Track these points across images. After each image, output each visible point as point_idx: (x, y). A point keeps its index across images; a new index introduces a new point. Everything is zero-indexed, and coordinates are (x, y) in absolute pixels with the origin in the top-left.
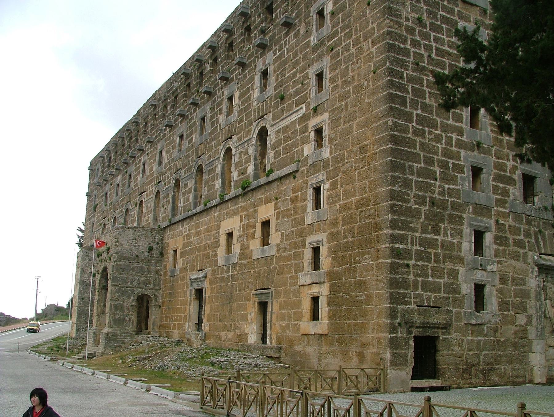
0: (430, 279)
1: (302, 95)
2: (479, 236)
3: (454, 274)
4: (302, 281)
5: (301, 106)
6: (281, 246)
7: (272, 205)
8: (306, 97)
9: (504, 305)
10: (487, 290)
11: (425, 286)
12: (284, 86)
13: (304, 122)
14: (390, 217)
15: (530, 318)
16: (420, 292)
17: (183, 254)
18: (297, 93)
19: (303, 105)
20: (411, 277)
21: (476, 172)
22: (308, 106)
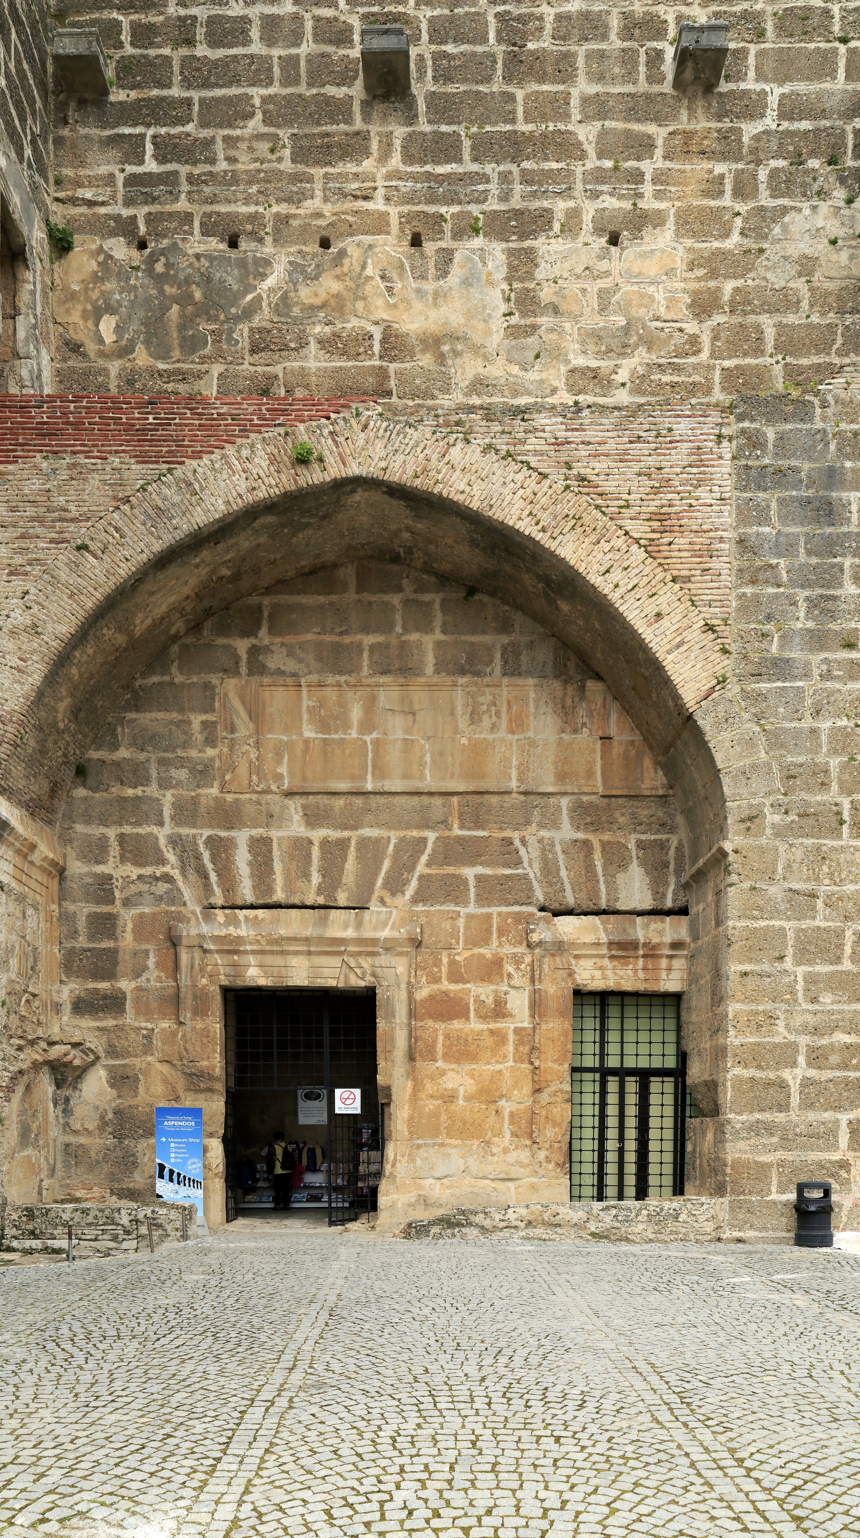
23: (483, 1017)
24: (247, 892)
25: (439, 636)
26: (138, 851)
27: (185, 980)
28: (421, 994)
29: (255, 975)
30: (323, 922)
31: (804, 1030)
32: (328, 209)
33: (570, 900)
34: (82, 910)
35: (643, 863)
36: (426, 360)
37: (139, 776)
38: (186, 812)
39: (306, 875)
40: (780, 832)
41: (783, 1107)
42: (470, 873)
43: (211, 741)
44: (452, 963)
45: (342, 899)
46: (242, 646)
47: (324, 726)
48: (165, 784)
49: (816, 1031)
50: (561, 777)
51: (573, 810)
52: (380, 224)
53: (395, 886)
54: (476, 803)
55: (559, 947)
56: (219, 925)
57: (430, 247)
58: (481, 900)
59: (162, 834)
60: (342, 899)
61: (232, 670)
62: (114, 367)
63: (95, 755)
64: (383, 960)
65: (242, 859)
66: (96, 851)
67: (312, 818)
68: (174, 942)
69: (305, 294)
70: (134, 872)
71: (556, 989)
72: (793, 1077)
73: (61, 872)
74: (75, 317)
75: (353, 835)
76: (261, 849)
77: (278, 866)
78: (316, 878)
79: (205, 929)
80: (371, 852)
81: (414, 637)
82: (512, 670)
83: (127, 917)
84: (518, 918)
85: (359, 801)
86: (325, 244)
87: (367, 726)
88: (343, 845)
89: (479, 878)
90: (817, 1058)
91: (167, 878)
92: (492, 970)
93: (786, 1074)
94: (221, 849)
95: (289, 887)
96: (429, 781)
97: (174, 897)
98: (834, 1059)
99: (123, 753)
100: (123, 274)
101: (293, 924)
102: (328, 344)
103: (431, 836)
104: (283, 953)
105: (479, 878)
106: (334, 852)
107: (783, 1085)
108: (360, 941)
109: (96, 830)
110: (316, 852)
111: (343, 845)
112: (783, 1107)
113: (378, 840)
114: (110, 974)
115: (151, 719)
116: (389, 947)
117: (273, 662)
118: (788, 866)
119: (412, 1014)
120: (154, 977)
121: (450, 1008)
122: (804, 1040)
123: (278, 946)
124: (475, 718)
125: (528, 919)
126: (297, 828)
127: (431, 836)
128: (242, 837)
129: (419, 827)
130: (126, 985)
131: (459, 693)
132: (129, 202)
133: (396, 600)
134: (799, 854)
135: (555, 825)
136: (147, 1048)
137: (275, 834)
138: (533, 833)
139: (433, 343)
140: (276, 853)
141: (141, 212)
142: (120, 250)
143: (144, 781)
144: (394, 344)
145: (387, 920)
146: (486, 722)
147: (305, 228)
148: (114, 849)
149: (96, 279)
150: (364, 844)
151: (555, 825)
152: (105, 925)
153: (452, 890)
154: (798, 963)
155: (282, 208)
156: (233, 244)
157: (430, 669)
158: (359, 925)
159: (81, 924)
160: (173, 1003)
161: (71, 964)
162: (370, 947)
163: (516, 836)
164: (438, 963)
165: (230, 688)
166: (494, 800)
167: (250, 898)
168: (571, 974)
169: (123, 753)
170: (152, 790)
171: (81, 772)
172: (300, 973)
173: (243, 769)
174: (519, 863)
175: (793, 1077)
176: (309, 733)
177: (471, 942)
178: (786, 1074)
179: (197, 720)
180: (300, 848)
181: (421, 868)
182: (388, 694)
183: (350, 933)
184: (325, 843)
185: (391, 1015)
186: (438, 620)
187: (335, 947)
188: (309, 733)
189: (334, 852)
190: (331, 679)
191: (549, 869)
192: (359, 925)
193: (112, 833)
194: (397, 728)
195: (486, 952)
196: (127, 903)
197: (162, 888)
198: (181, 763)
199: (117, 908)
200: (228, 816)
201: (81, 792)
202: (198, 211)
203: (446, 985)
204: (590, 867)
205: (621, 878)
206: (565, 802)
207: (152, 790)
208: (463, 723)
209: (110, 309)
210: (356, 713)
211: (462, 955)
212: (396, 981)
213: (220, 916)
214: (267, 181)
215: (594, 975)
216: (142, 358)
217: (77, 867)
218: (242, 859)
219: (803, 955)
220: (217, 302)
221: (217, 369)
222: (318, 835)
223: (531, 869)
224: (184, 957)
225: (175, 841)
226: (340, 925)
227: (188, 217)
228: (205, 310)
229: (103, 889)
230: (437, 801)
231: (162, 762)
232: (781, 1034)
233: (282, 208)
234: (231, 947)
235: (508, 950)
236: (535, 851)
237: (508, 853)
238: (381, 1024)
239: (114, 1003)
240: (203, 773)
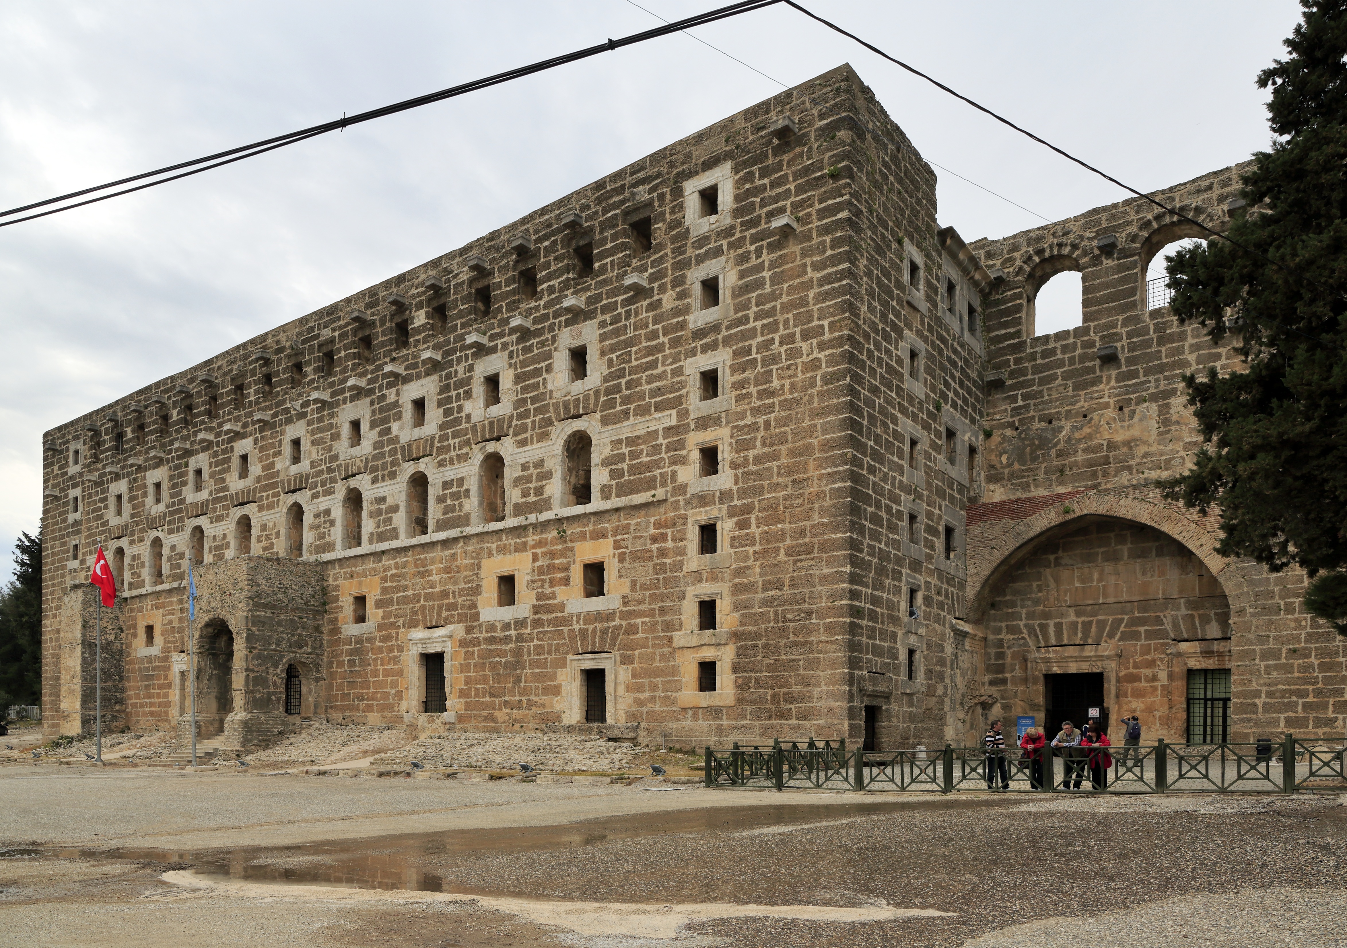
0: (877, 642)
1: (671, 396)
2: (913, 592)
3: (894, 637)
4: (675, 644)
5: (668, 412)
6: (630, 598)
7: (611, 540)
8: (679, 401)
9: (929, 672)
10: (917, 656)
11: (878, 651)
12: (628, 378)
13: (676, 434)
14: (848, 569)
15: (946, 688)
16: (870, 656)
17: (379, 604)
18: (658, 391)
19: (674, 412)
20: (865, 640)
21: (913, 518)
22: (683, 415)
23: (1147, 680)
24: (1053, 641)
25: (1129, 545)
26: (1013, 630)
27: (1029, 672)
28: (1122, 674)
29: (1056, 670)
30: (1083, 650)
31: (1265, 684)
32: (1086, 405)
33: (1185, 636)
34: (993, 651)
35: (1217, 621)
36: (1125, 450)
37: (1014, 605)
38: (1030, 616)
39: (1076, 634)
40: (1253, 615)
41: (1256, 712)
42: (1142, 629)
43: (1040, 591)
44: (1135, 662)
45: (1090, 641)
46: (1052, 557)
47: (1083, 582)
48: (1022, 607)
49: (1270, 685)
50: (1181, 591)
51: (1185, 604)
52: (1107, 406)
53: (1111, 635)
54: (1144, 604)
55: (1179, 655)
56: (1043, 654)
57: (1126, 410)
58: (1146, 639)
59: (1021, 624)
60: (1090, 641)
61: (1048, 566)
62: (1006, 471)
63: (998, 599)
64: (1106, 662)
65: (1051, 630)
66: (998, 631)
67: (1078, 614)
68: (1025, 660)
69: (1077, 435)
70: (1011, 637)
72: (1260, 702)
73: (985, 639)
74: (993, 457)
75: (1095, 619)
76: (1059, 626)
77: (1065, 632)
78: (1080, 635)
79: (1037, 655)
80: (1101, 625)
81: (1119, 547)
82: (1158, 555)
83: (1009, 653)
84: (1162, 644)
86: (1085, 416)
87: (1100, 580)
88: (1090, 623)
90: (1270, 694)
91: (1023, 638)
92: (1151, 664)
93: (1257, 701)
94: (1044, 628)
95: (1069, 639)
96: (1125, 597)
97: (1026, 644)
98: (1278, 695)
99: (1008, 598)
100: (1010, 440)
101: (1071, 651)
102: (1085, 451)
103: (1126, 617)
106: (1087, 626)
107: (1255, 705)
109: (998, 624)
110: (1080, 626)
111: (1090, 623)
112: (1256, 712)
114: (1002, 672)
115: (1019, 585)
116: (1108, 657)
117: (1063, 562)
118: (1257, 627)
119: (1118, 680)
120: (1018, 672)
121: (1134, 678)
122: (1264, 689)
123: (1065, 660)
124: (1144, 573)
125: (1167, 644)
126: (1073, 618)
127: (1126, 617)
128: (1051, 623)
130: (1008, 675)
131: (1138, 565)
132: (1012, 416)
133: (1112, 535)
134: (1261, 622)
135: (1178, 609)
136: (1016, 695)
137: (1064, 621)
138: (1169, 613)
139: (1127, 443)
141: (1016, 419)
142: (1009, 432)
143: (1016, 606)
144: (1112, 446)
145: (1108, 648)
146: (1149, 574)
147: (1077, 413)
148: (1004, 630)
149: (1000, 443)
150: (1098, 622)
151: (1178, 609)
152: (1000, 655)
153: (1135, 636)
154: (1261, 661)
155: (1069, 408)
156: (1050, 422)
157: (1126, 558)
158: (1096, 650)
159: (992, 655)
160: (1025, 681)
161: (988, 669)
162: (1101, 658)
163: (1161, 615)
165: (1048, 572)
168: (1186, 664)
169: (1008, 598)
170: (1018, 609)
171: (993, 606)
172: (1073, 668)
173: (1052, 599)
174: (1163, 624)
175: (1260, 702)
176: (1077, 585)
177: (1142, 654)
178: (1257, 701)
179: (1035, 584)
180: (1074, 625)
181: (1122, 629)
182: (1109, 568)
183: (1093, 654)
184: (1083, 622)
185: (1109, 681)
186: (1129, 540)
187: (1087, 659)
188: (1077, 585)
189: (1087, 626)
190: (1086, 565)
191: (1176, 626)
192: (1096, 650)
193: (1003, 625)
194: (1112, 580)
195: (1149, 657)
196: (1009, 647)
197: (1022, 642)
198: (1029, 599)
199: (1005, 649)
200: (1046, 616)
201: (993, 612)
202: (1037, 415)
203: (1132, 670)
204: (1193, 624)
205: (1207, 627)
206: (1182, 601)
207: (1018, 609)
208: (1139, 575)
209: (1005, 452)
210: (1096, 576)
211: (1139, 659)
212: (1111, 669)
213: (1043, 650)
214: (1063, 400)
215: (1194, 664)
216: (1016, 466)
217: (991, 637)
218: (1051, 630)
219: (1263, 658)
220: (1044, 443)
221: (1043, 465)
222: (1080, 620)
223: (1169, 627)
224: (1029, 665)
225: (1026, 626)
226: (1089, 651)
227: (1034, 417)
228: (1040, 447)
229: (1000, 643)
231: (1022, 600)
232: (1254, 686)
233: (1069, 408)
234: (1047, 661)
235: (1158, 656)
236: (1170, 619)
237: (1158, 621)
238: (1105, 685)
239: (1004, 681)
240: (1037, 602)
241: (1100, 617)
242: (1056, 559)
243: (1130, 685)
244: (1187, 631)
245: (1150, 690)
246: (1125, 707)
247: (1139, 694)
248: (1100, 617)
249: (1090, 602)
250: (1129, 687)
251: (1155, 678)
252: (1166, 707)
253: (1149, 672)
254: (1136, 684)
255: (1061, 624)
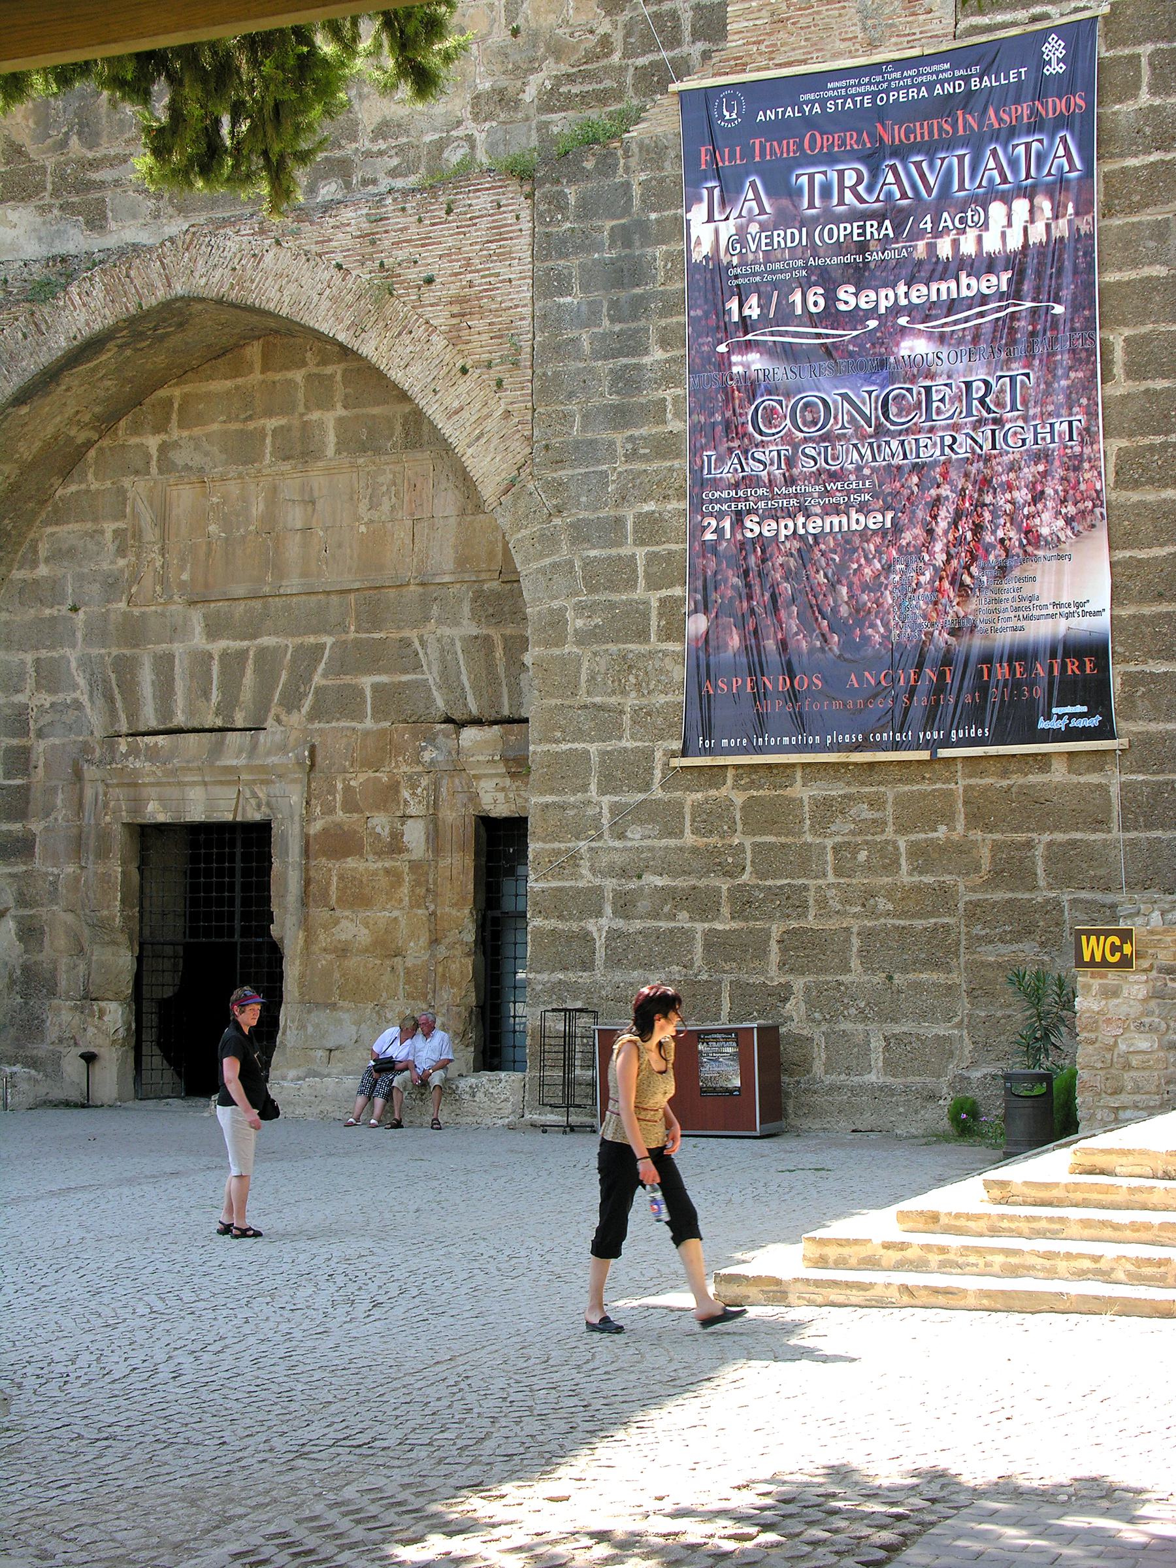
28: (316, 827)
39: (206, 694)
42: (367, 682)
44: (347, 789)
46: (153, 442)
50: (462, 562)
53: (291, 702)
61: (141, 471)
71: (456, 816)
78: (215, 696)
85: (258, 604)
89: (376, 688)
104: (181, 784)
105: (376, 688)
108: (250, 769)
111: (242, 655)
113: (276, 649)
126: (199, 640)
127: (329, 640)
129: (316, 632)
137: (178, 648)
140: (178, 670)
164: (332, 790)
166: (392, 593)
167: (153, 724)
168: (474, 797)
174: (417, 667)
179: (109, 527)
181: (318, 679)
184: (224, 655)
187: (230, 776)
203: (340, 815)
223: (431, 676)
230: (335, 599)
241: (267, 641)
242: (163, 448)
243: (335, 866)
244: (478, 695)
245: (384, 882)
246: (323, 939)
247: (358, 896)
248: (267, 641)
249: (240, 591)
250: (332, 870)
251: (396, 846)
252: (424, 940)
253: (381, 823)
254: (351, 863)
255: (169, 658)
